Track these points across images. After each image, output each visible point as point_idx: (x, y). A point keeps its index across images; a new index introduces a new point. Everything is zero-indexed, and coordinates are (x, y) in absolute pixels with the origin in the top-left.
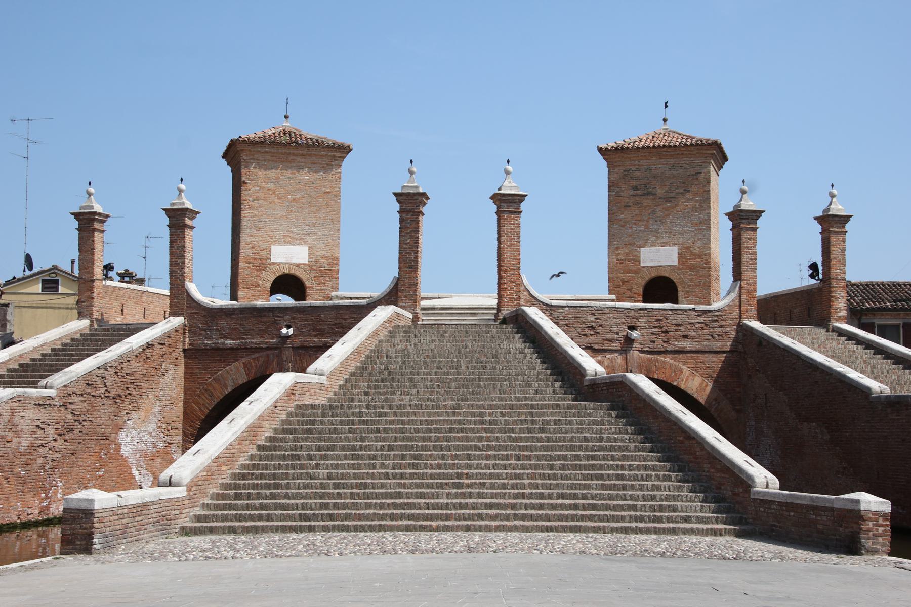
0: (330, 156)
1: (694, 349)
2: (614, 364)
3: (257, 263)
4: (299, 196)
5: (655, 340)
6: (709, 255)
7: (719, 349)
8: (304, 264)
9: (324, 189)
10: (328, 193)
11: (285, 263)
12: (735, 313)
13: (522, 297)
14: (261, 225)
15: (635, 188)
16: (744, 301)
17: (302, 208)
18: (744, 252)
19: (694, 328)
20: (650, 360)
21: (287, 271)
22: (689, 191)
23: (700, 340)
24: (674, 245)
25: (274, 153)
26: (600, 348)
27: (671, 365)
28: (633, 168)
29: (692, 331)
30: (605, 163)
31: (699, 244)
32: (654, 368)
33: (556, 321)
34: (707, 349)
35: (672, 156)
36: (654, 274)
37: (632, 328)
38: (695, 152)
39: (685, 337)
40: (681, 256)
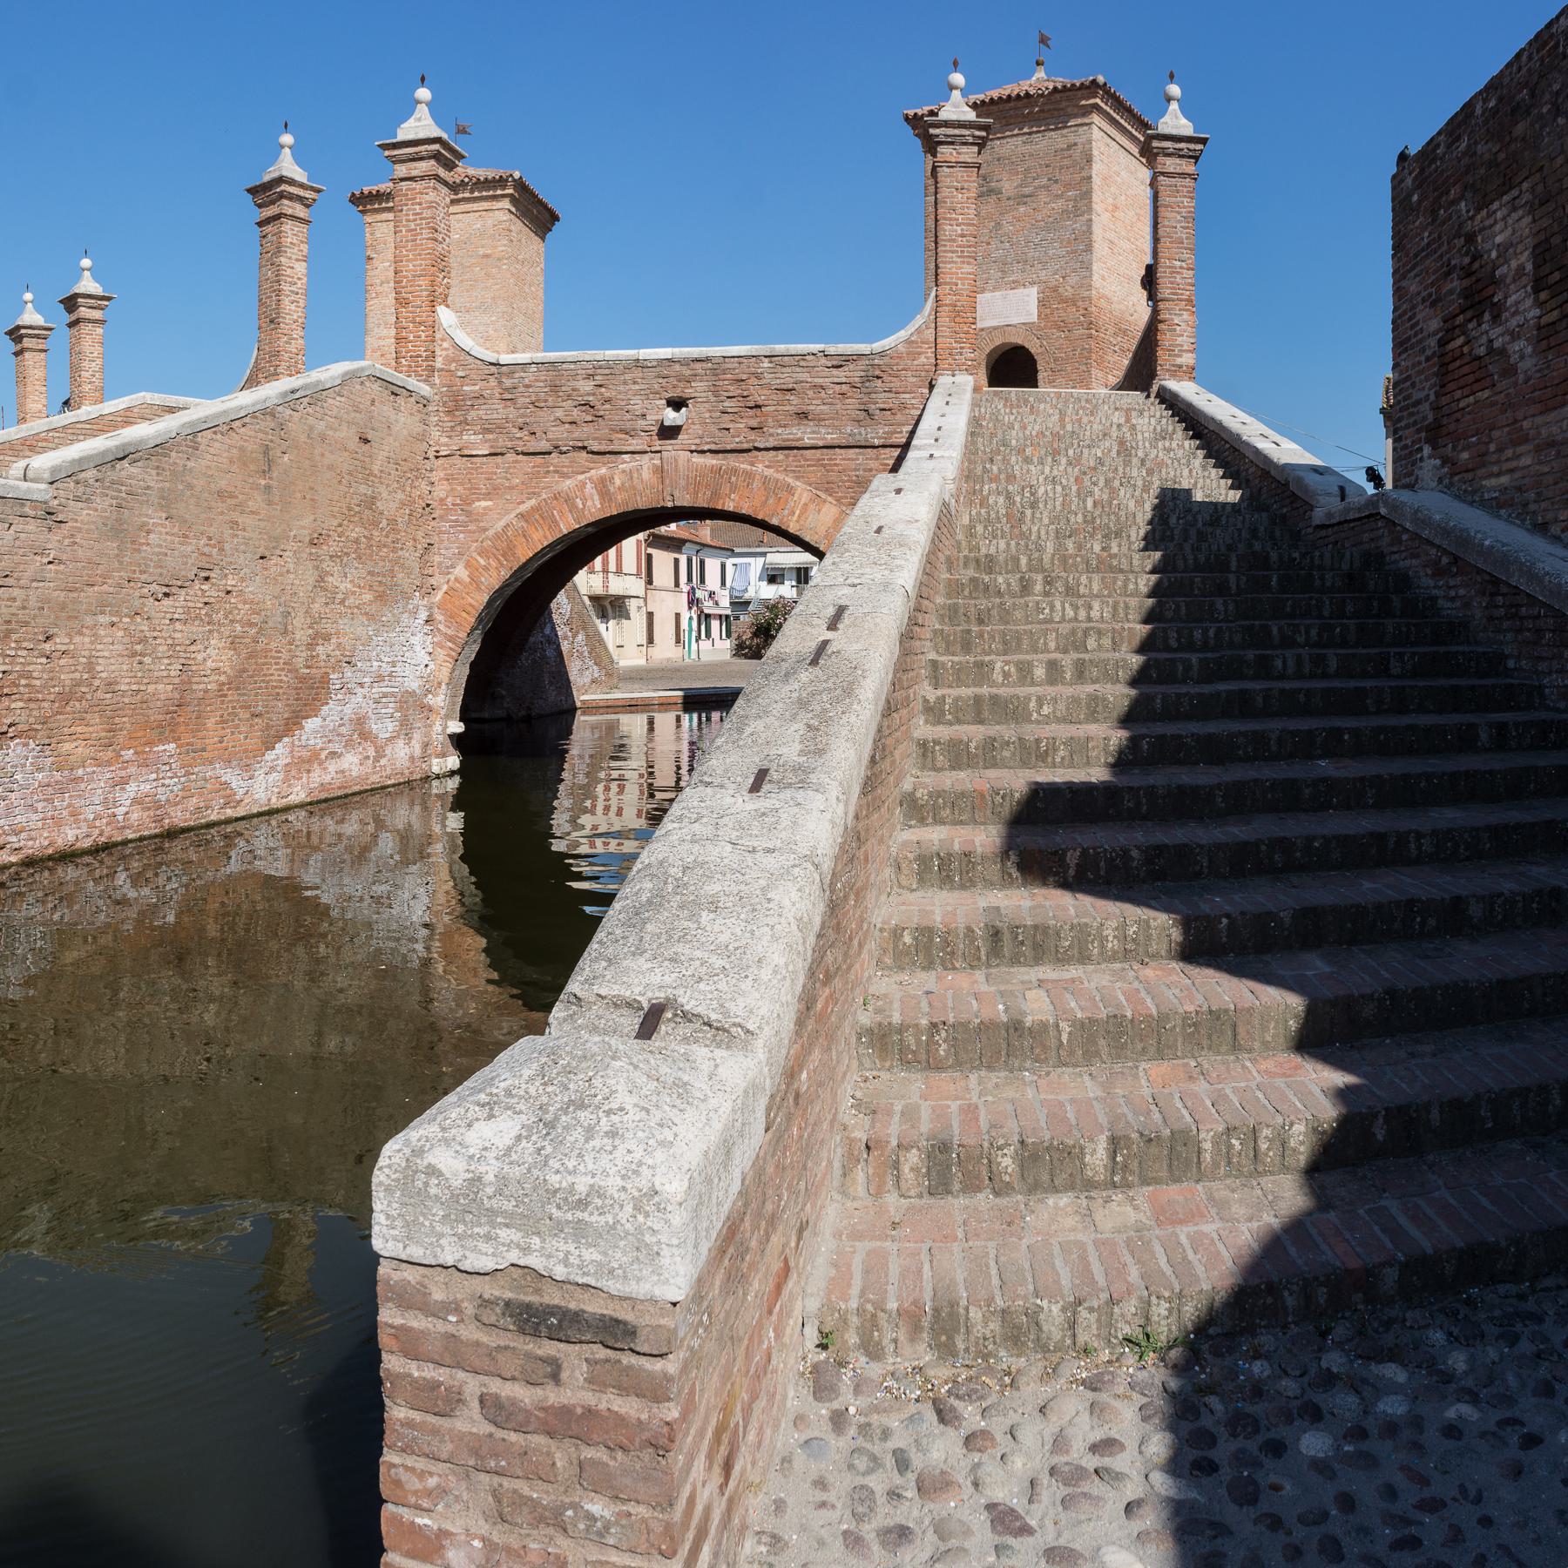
1: (821, 443)
2: (636, 481)
5: (730, 426)
7: (882, 442)
12: (923, 359)
13: (438, 352)
16: (944, 331)
18: (945, 219)
19: (823, 394)
20: (718, 471)
23: (836, 423)
26: (603, 448)
27: (766, 480)
29: (819, 402)
32: (726, 489)
33: (510, 396)
34: (852, 442)
37: (677, 404)
39: (803, 416)
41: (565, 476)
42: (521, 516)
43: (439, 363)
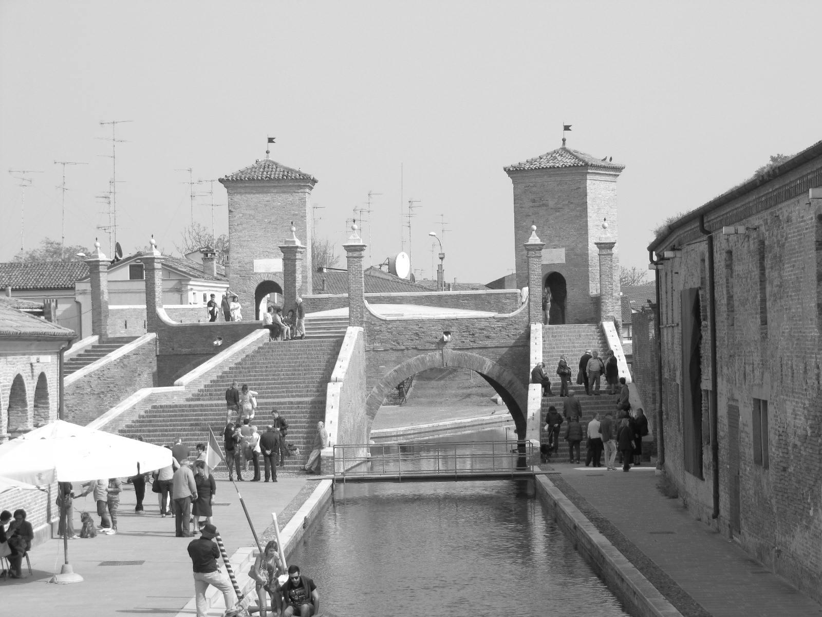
0: (295, 186)
3: (243, 273)
4: (273, 218)
6: (587, 255)
8: (280, 273)
9: (293, 212)
10: (296, 215)
11: (264, 273)
14: (245, 244)
15: (534, 201)
17: (276, 228)
21: (266, 279)
22: (572, 203)
24: (563, 247)
25: (252, 187)
26: (422, 348)
28: (531, 185)
30: (510, 180)
31: (580, 246)
35: (558, 174)
36: (549, 271)
38: (573, 172)
40: (567, 255)
41: (410, 357)
42: (395, 371)
43: (365, 319)
